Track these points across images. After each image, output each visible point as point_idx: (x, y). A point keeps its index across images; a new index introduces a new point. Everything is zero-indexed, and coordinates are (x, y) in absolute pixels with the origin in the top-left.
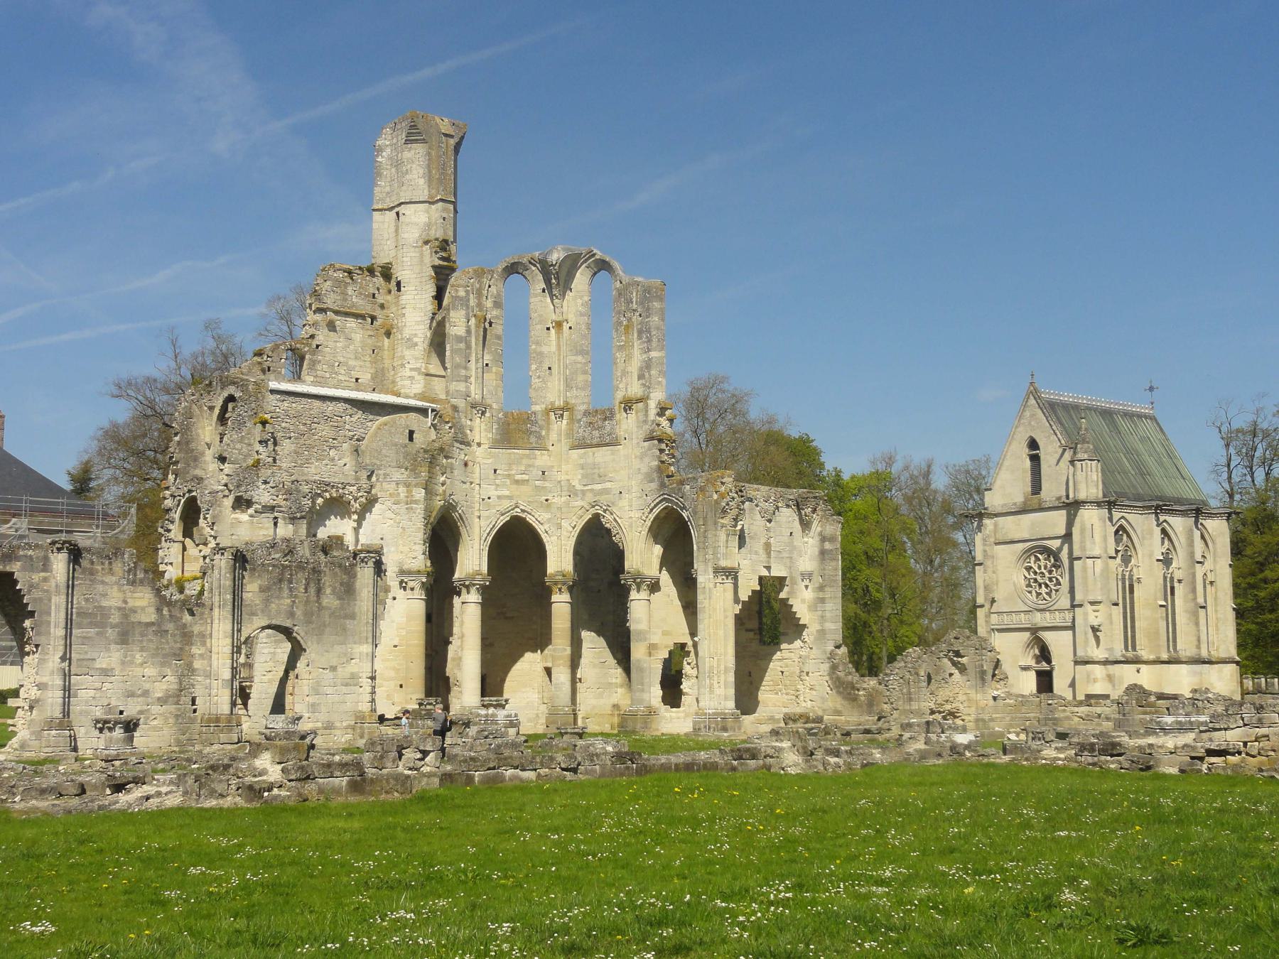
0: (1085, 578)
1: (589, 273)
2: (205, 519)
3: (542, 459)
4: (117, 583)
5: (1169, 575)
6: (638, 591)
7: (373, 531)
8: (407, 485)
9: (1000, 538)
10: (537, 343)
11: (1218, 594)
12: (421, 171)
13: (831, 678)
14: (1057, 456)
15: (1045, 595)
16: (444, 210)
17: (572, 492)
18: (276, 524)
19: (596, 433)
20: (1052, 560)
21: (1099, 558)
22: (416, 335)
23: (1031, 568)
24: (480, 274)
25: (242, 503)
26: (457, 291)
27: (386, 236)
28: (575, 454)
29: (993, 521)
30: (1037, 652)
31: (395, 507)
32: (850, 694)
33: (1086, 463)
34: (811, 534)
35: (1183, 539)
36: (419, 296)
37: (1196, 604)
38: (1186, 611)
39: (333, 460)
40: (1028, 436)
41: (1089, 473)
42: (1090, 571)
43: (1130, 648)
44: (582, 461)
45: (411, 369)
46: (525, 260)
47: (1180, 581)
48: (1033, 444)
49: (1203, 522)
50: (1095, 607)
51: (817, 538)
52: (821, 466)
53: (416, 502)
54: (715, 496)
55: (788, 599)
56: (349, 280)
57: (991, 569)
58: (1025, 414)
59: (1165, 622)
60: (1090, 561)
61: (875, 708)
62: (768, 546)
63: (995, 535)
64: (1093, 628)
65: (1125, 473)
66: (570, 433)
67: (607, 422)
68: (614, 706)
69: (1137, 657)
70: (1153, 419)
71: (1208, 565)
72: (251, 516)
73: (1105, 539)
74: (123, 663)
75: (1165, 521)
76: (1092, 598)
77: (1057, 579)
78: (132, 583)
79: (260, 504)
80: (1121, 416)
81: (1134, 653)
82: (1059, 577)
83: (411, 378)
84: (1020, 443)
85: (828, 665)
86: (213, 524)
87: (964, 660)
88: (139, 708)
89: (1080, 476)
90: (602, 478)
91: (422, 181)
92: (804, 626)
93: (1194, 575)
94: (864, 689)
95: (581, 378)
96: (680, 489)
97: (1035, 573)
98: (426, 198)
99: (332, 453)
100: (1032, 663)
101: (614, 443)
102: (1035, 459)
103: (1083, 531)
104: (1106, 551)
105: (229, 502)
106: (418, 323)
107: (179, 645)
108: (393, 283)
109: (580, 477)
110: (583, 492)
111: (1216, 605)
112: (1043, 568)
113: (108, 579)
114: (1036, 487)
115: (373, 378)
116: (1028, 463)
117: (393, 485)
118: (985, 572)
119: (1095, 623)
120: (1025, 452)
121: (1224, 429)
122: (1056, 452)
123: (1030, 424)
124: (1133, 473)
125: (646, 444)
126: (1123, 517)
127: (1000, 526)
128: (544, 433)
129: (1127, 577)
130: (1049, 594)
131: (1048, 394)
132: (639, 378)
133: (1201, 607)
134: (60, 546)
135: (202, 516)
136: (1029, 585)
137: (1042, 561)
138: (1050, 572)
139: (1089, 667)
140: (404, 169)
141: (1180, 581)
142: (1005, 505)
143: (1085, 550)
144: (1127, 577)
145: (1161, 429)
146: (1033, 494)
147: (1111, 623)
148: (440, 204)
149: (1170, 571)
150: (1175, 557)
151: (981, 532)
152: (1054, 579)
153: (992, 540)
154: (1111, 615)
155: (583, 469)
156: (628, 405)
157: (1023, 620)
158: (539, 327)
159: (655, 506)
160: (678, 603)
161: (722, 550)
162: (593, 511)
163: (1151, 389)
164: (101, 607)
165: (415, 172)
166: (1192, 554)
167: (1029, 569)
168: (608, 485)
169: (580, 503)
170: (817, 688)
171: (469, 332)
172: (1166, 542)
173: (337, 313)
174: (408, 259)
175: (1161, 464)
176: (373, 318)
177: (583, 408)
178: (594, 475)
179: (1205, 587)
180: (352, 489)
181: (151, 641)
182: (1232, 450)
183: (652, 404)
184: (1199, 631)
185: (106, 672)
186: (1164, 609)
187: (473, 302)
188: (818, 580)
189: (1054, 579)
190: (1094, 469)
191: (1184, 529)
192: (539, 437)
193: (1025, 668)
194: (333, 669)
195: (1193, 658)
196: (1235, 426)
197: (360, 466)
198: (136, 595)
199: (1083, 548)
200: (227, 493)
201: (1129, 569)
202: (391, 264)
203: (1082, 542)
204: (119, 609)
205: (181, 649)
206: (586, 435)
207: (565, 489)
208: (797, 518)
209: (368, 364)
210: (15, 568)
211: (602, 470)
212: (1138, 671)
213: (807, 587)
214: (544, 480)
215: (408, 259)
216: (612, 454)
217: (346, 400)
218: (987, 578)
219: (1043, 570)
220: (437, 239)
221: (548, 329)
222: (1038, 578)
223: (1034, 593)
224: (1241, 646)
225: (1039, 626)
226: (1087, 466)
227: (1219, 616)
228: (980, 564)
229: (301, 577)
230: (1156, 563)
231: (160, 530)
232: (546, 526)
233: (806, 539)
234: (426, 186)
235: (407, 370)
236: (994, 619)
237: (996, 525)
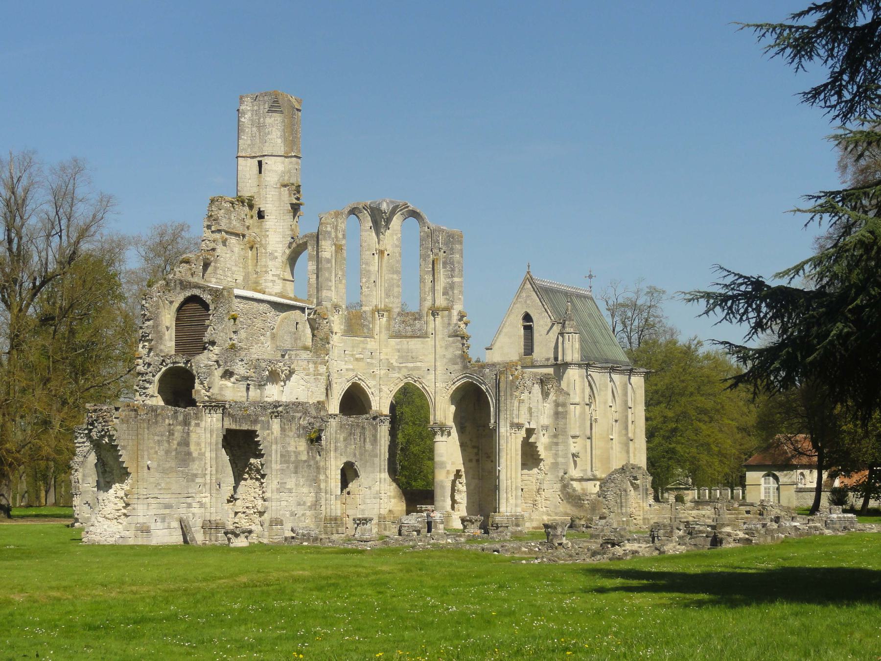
1: (402, 218)
2: (202, 383)
3: (371, 344)
4: (293, 436)
6: (442, 436)
7: (291, 393)
8: (315, 363)
10: (367, 264)
12: (279, 134)
13: (562, 493)
16: (297, 163)
17: (390, 368)
18: (248, 389)
19: (409, 328)
22: (276, 251)
24: (337, 215)
25: (228, 374)
26: (326, 227)
27: (248, 176)
28: (393, 341)
31: (306, 377)
32: (578, 503)
34: (548, 401)
36: (278, 224)
37: (628, 438)
38: (620, 443)
39: (262, 343)
44: (399, 347)
45: (273, 275)
46: (361, 207)
48: (527, 317)
51: (553, 404)
53: (321, 375)
54: (511, 378)
55: (536, 443)
56: (232, 209)
58: (521, 295)
61: (597, 512)
62: (530, 409)
64: (573, 455)
66: (388, 328)
68: (390, 511)
69: (593, 475)
70: (592, 299)
72: (234, 383)
74: (296, 485)
78: (299, 437)
79: (239, 375)
83: (273, 281)
85: (559, 485)
86: (210, 388)
87: (638, 482)
88: (302, 512)
89: (567, 344)
90: (414, 359)
91: (279, 141)
92: (542, 460)
93: (627, 417)
94: (587, 500)
95: (396, 290)
96: (480, 372)
98: (282, 154)
99: (262, 338)
101: (424, 336)
102: (528, 329)
104: (584, 400)
105: (218, 372)
106: (278, 242)
107: (315, 474)
108: (255, 212)
109: (397, 357)
110: (400, 368)
113: (291, 434)
114: (529, 348)
115: (244, 280)
116: (522, 331)
117: (305, 363)
119: (574, 450)
120: (520, 324)
123: (526, 302)
128: (371, 326)
131: (546, 280)
132: (444, 294)
134: (276, 414)
135: (197, 381)
140: (267, 130)
145: (597, 307)
146: (525, 355)
147: (586, 452)
148: (294, 159)
154: (586, 445)
155: (399, 352)
156: (434, 312)
158: (368, 253)
159: (458, 380)
160: (458, 443)
161: (515, 412)
162: (406, 381)
164: (288, 451)
165: (274, 133)
166: (626, 402)
168: (419, 364)
169: (397, 375)
170: (551, 499)
171: (332, 256)
173: (227, 232)
174: (271, 196)
175: (602, 334)
176: (244, 236)
177: (397, 310)
178: (406, 356)
180: (281, 364)
181: (305, 471)
182: (617, 318)
183: (455, 313)
184: (629, 457)
185: (290, 491)
187: (333, 235)
188: (552, 431)
190: (577, 340)
192: (369, 329)
194: (370, 488)
197: (277, 348)
198: (300, 443)
200: (217, 366)
202: (253, 197)
204: (295, 452)
205: (316, 476)
207: (386, 365)
208: (540, 391)
209: (242, 270)
210: (258, 427)
211: (414, 354)
213: (544, 435)
214: (372, 358)
215: (271, 196)
216: (423, 343)
217: (269, 302)
220: (293, 184)
221: (373, 254)
229: (358, 431)
231: (136, 387)
232: (373, 390)
233: (545, 404)
234: (282, 145)
235: (270, 275)
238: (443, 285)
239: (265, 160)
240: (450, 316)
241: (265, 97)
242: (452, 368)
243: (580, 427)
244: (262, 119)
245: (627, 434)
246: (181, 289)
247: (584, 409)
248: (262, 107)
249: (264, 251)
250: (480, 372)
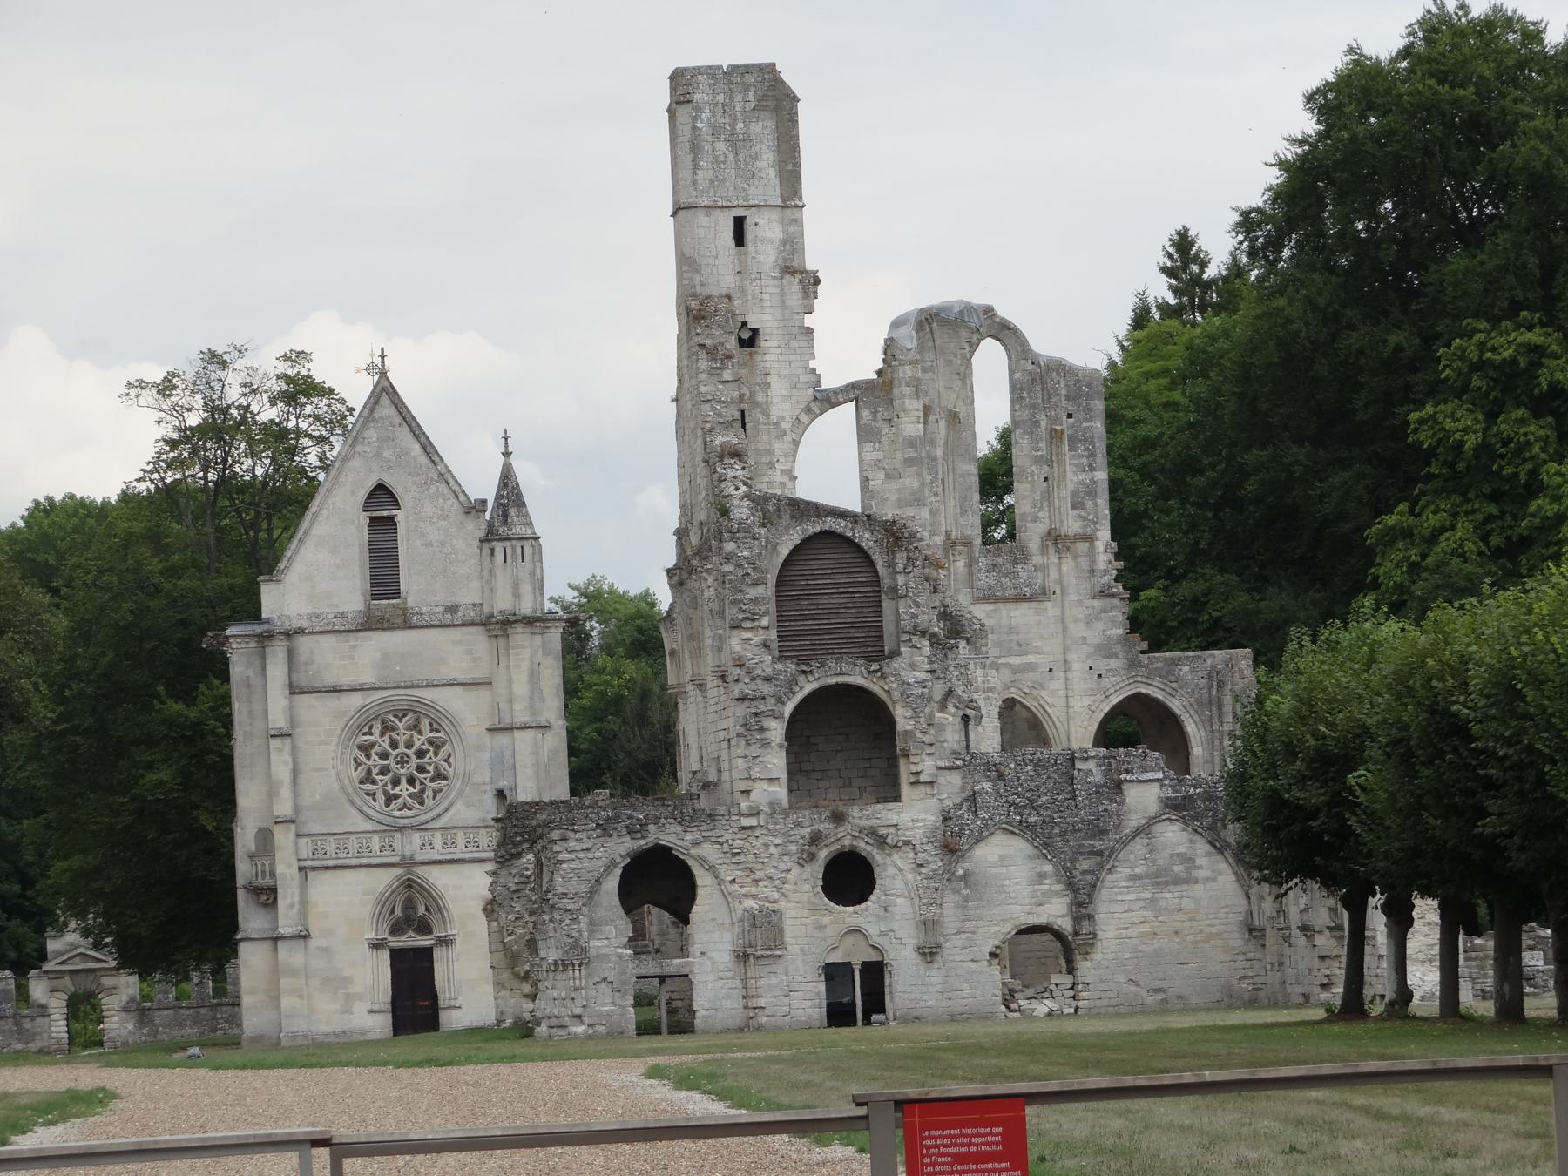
19: (1005, 581)
40: (370, 484)
67: (1020, 567)
84: (353, 492)
101: (1038, 596)
112: (402, 744)
123: (378, 455)
125: (1097, 603)
132: (1073, 508)
136: (368, 778)
193: (376, 946)
206: (992, 582)
216: (1037, 614)
223: (381, 797)
238: (1071, 487)
239: (752, 217)
240: (1092, 554)
241: (747, 76)
242: (1102, 665)
244: (740, 125)
246: (793, 517)
248: (739, 98)
249: (762, 418)
250: (1171, 673)
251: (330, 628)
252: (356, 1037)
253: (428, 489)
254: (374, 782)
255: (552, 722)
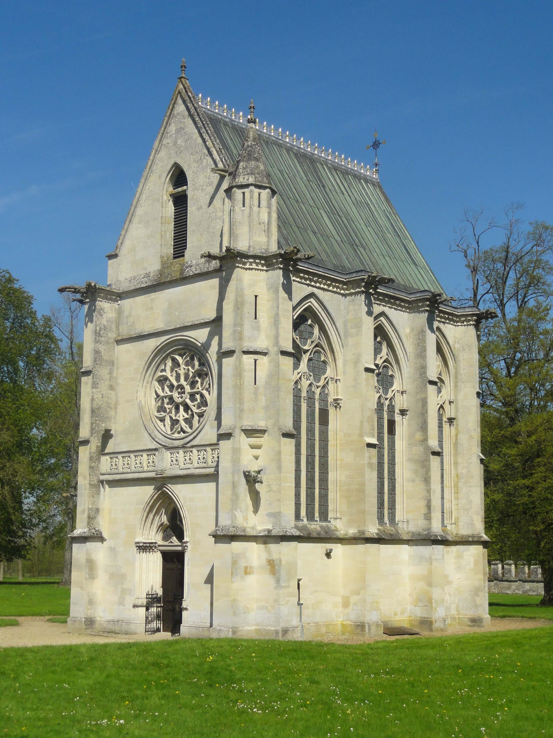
0: (239, 387)
5: (387, 402)
9: (125, 332)
11: (460, 436)
14: (211, 190)
15: (183, 424)
20: (197, 363)
21: (265, 354)
23: (166, 379)
29: (115, 305)
30: (164, 519)
33: (251, 191)
35: (410, 347)
37: (427, 448)
38: (409, 460)
41: (255, 208)
42: (248, 376)
43: (317, 515)
47: (403, 412)
49: (441, 326)
50: (253, 441)
52: (33, 314)
57: (107, 383)
59: (375, 474)
60: (248, 360)
63: (118, 328)
65: (326, 237)
69: (327, 530)
71: (447, 393)
73: (276, 321)
75: (383, 314)
76: (248, 423)
77: (202, 396)
80: (329, 169)
81: (324, 524)
82: (205, 392)
84: (160, 177)
89: (241, 214)
93: (424, 402)
97: (171, 387)
100: (157, 538)
103: (239, 306)
104: (277, 343)
111: (456, 454)
116: (170, 209)
118: (95, 385)
119: (253, 467)
121: (470, 252)
122: (210, 184)
123: (175, 143)
124: (338, 238)
126: (312, 295)
127: (126, 314)
129: (317, 397)
130: (189, 421)
133: (435, 453)
136: (161, 409)
137: (183, 366)
138: (193, 384)
139: (236, 545)
141: (403, 412)
142: (134, 278)
143: (241, 339)
144: (317, 397)
147: (279, 468)
149: (389, 395)
150: (397, 375)
151: (92, 321)
152: (198, 397)
153: (112, 335)
154: (279, 453)
157: (145, 465)
163: (376, 145)
166: (423, 369)
167: (162, 381)
172: (385, 349)
179: (440, 426)
184: (429, 491)
186: (374, 451)
189: (198, 397)
190: (264, 203)
191: (412, 330)
195: (419, 534)
196: (485, 246)
199: (239, 336)
201: (321, 384)
203: (238, 324)
212: (328, 555)
218: (98, 396)
219: (183, 382)
222: (175, 395)
223: (168, 421)
224: (489, 525)
225: (168, 473)
226: (252, 197)
227: (460, 470)
228: (87, 373)
230: (364, 374)
236: (105, 463)
237: (120, 312)
243: (267, 408)
245: (425, 440)
247: (278, 365)
251: (138, 286)
252: (125, 627)
253: (202, 163)
254: (165, 411)
255: (270, 349)
